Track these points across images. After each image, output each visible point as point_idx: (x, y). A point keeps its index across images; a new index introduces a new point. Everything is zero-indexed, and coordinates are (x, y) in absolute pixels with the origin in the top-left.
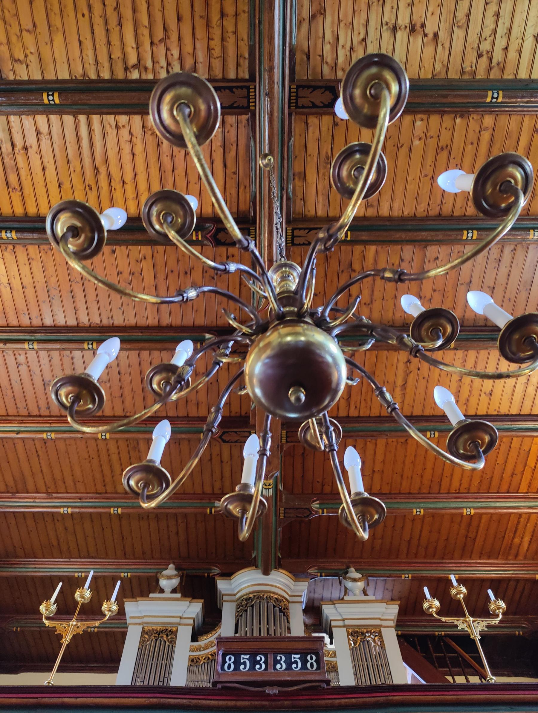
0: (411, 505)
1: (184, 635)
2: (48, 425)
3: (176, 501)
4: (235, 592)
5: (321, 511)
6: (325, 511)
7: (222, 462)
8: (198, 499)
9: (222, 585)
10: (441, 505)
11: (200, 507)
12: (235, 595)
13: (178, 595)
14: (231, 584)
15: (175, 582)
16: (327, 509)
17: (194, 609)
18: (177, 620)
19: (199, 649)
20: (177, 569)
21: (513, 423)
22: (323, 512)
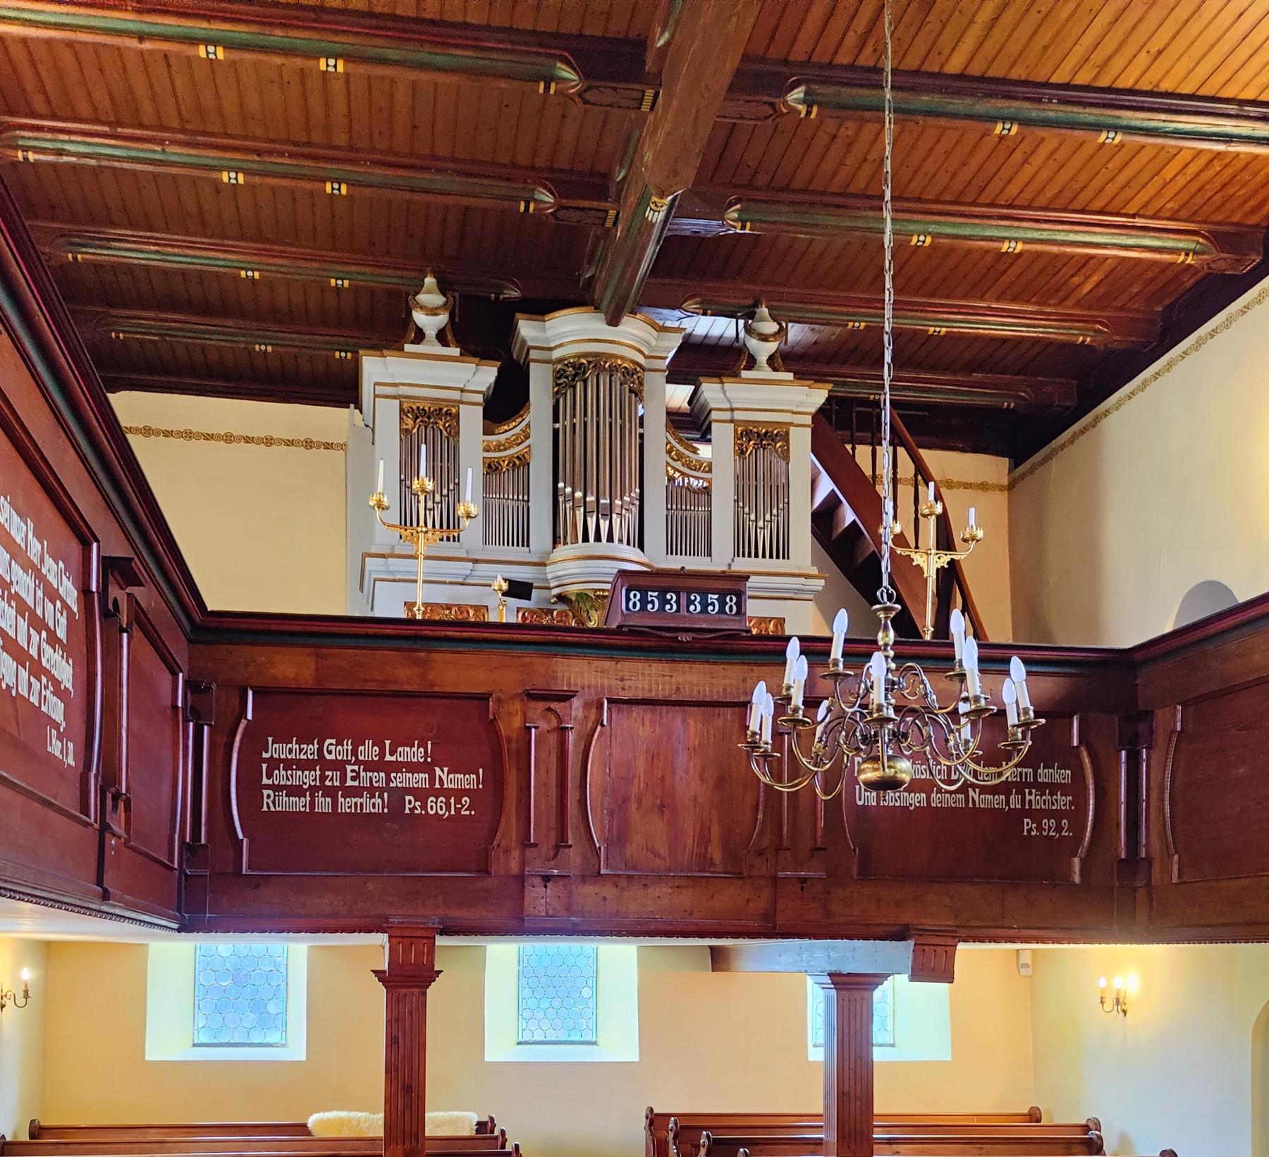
0: (912, 227)
1: (472, 418)
2: (205, 25)
3: (457, 179)
4: (552, 345)
5: (739, 225)
6: (748, 225)
7: (564, 116)
8: (501, 178)
9: (527, 329)
10: (967, 231)
11: (506, 198)
12: (550, 349)
14: (544, 330)
16: (751, 221)
17: (485, 376)
18: (455, 395)
19: (498, 448)
21: (1169, 117)
22: (743, 228)
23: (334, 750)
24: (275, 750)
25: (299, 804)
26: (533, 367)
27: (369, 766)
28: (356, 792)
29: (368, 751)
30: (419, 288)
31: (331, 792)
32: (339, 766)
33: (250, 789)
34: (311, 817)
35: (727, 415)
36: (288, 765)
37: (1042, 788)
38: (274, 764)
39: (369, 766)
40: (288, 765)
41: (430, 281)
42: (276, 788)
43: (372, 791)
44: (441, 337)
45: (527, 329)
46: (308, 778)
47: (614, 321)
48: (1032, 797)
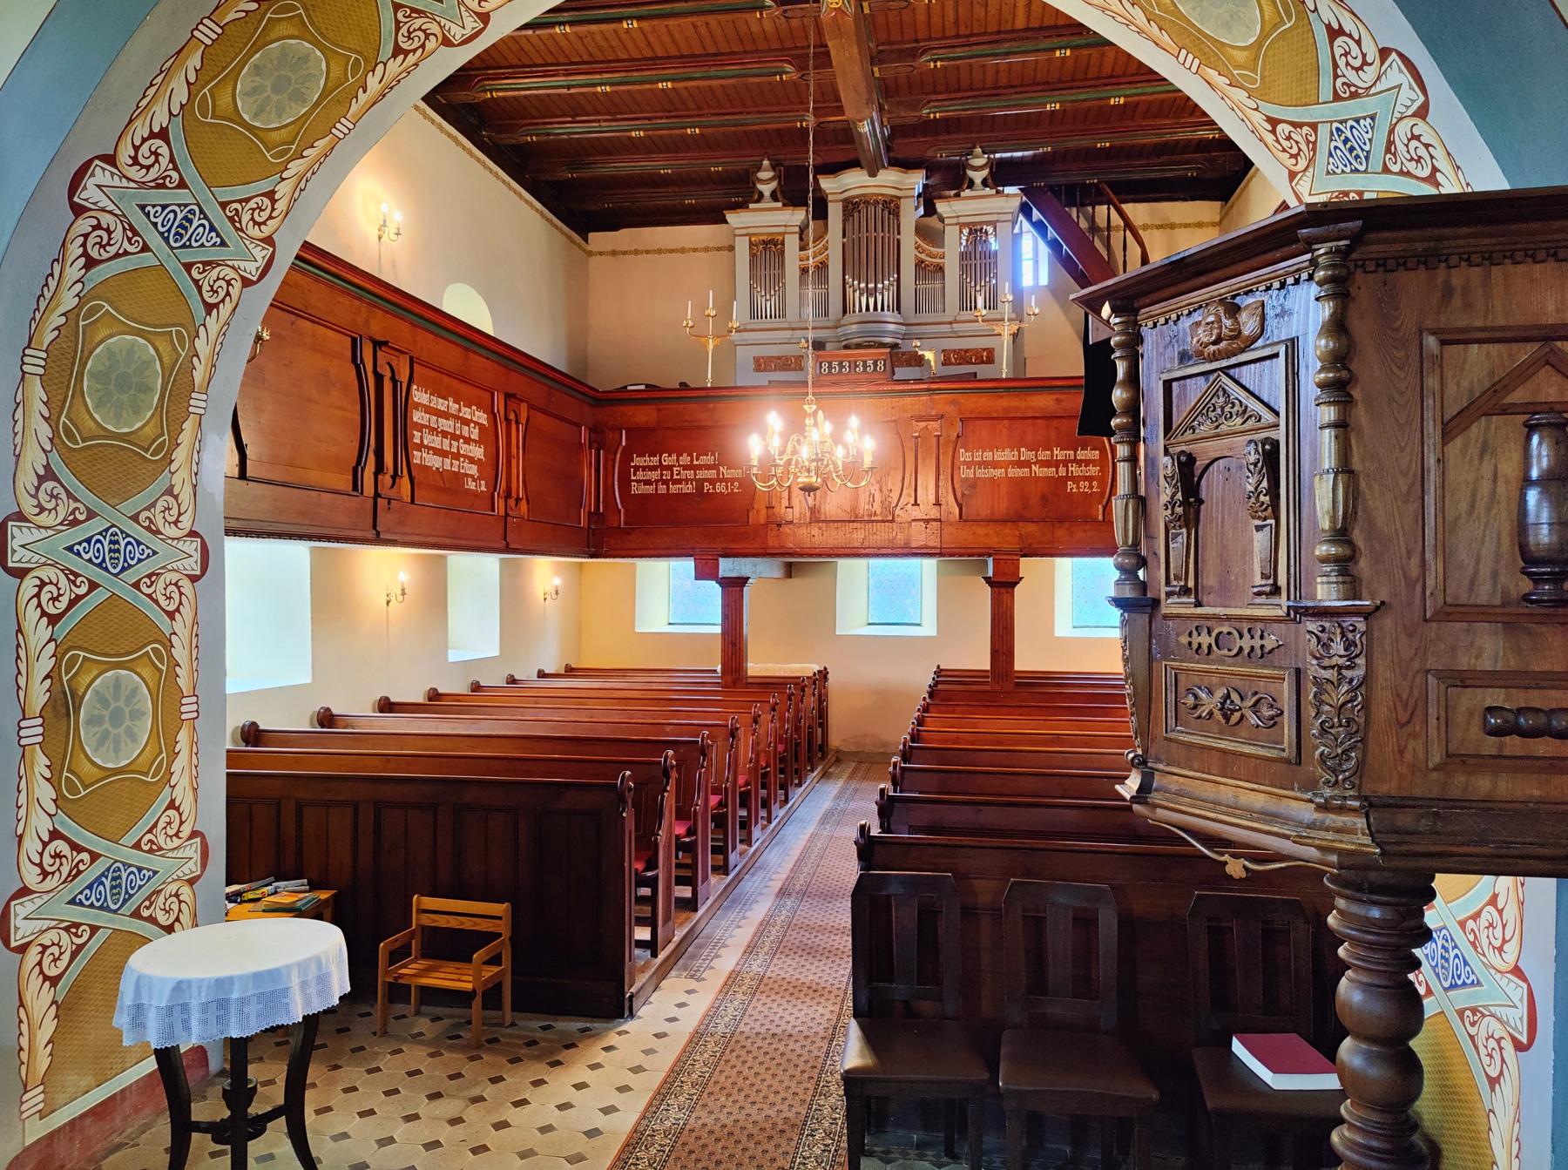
1: (792, 243)
13: (779, 204)
15: (774, 185)
17: (798, 216)
20: (773, 168)
23: (667, 460)
24: (638, 461)
25: (650, 489)
26: (831, 206)
27: (686, 468)
28: (679, 482)
29: (685, 459)
30: (759, 168)
31: (666, 482)
32: (670, 468)
33: (625, 482)
34: (656, 495)
35: (954, 221)
36: (644, 468)
37: (1079, 463)
38: (637, 468)
39: (686, 468)
40: (644, 468)
41: (766, 163)
42: (638, 481)
43: (687, 481)
44: (774, 197)
45: (827, 183)
46: (654, 475)
47: (873, 174)
48: (1073, 468)
